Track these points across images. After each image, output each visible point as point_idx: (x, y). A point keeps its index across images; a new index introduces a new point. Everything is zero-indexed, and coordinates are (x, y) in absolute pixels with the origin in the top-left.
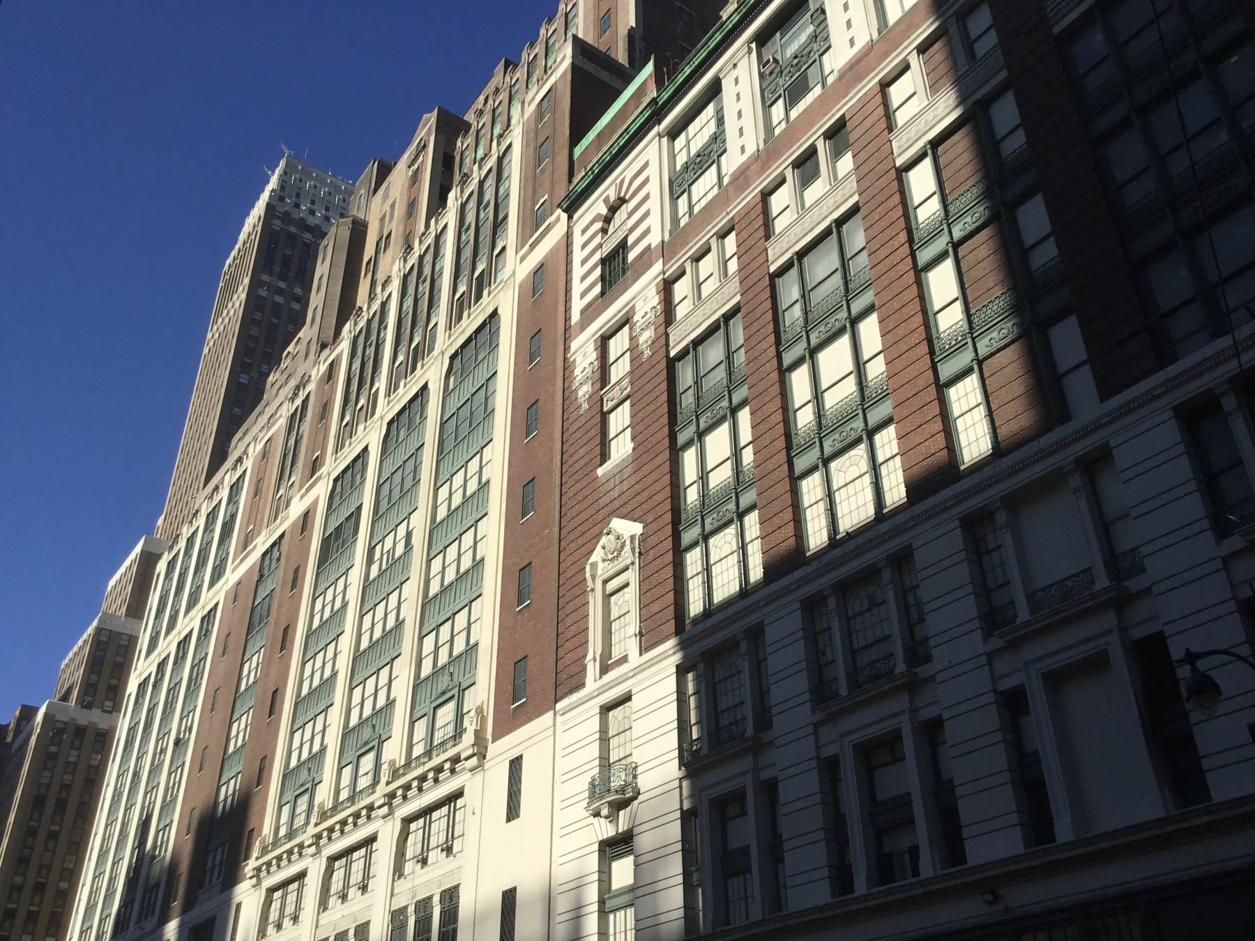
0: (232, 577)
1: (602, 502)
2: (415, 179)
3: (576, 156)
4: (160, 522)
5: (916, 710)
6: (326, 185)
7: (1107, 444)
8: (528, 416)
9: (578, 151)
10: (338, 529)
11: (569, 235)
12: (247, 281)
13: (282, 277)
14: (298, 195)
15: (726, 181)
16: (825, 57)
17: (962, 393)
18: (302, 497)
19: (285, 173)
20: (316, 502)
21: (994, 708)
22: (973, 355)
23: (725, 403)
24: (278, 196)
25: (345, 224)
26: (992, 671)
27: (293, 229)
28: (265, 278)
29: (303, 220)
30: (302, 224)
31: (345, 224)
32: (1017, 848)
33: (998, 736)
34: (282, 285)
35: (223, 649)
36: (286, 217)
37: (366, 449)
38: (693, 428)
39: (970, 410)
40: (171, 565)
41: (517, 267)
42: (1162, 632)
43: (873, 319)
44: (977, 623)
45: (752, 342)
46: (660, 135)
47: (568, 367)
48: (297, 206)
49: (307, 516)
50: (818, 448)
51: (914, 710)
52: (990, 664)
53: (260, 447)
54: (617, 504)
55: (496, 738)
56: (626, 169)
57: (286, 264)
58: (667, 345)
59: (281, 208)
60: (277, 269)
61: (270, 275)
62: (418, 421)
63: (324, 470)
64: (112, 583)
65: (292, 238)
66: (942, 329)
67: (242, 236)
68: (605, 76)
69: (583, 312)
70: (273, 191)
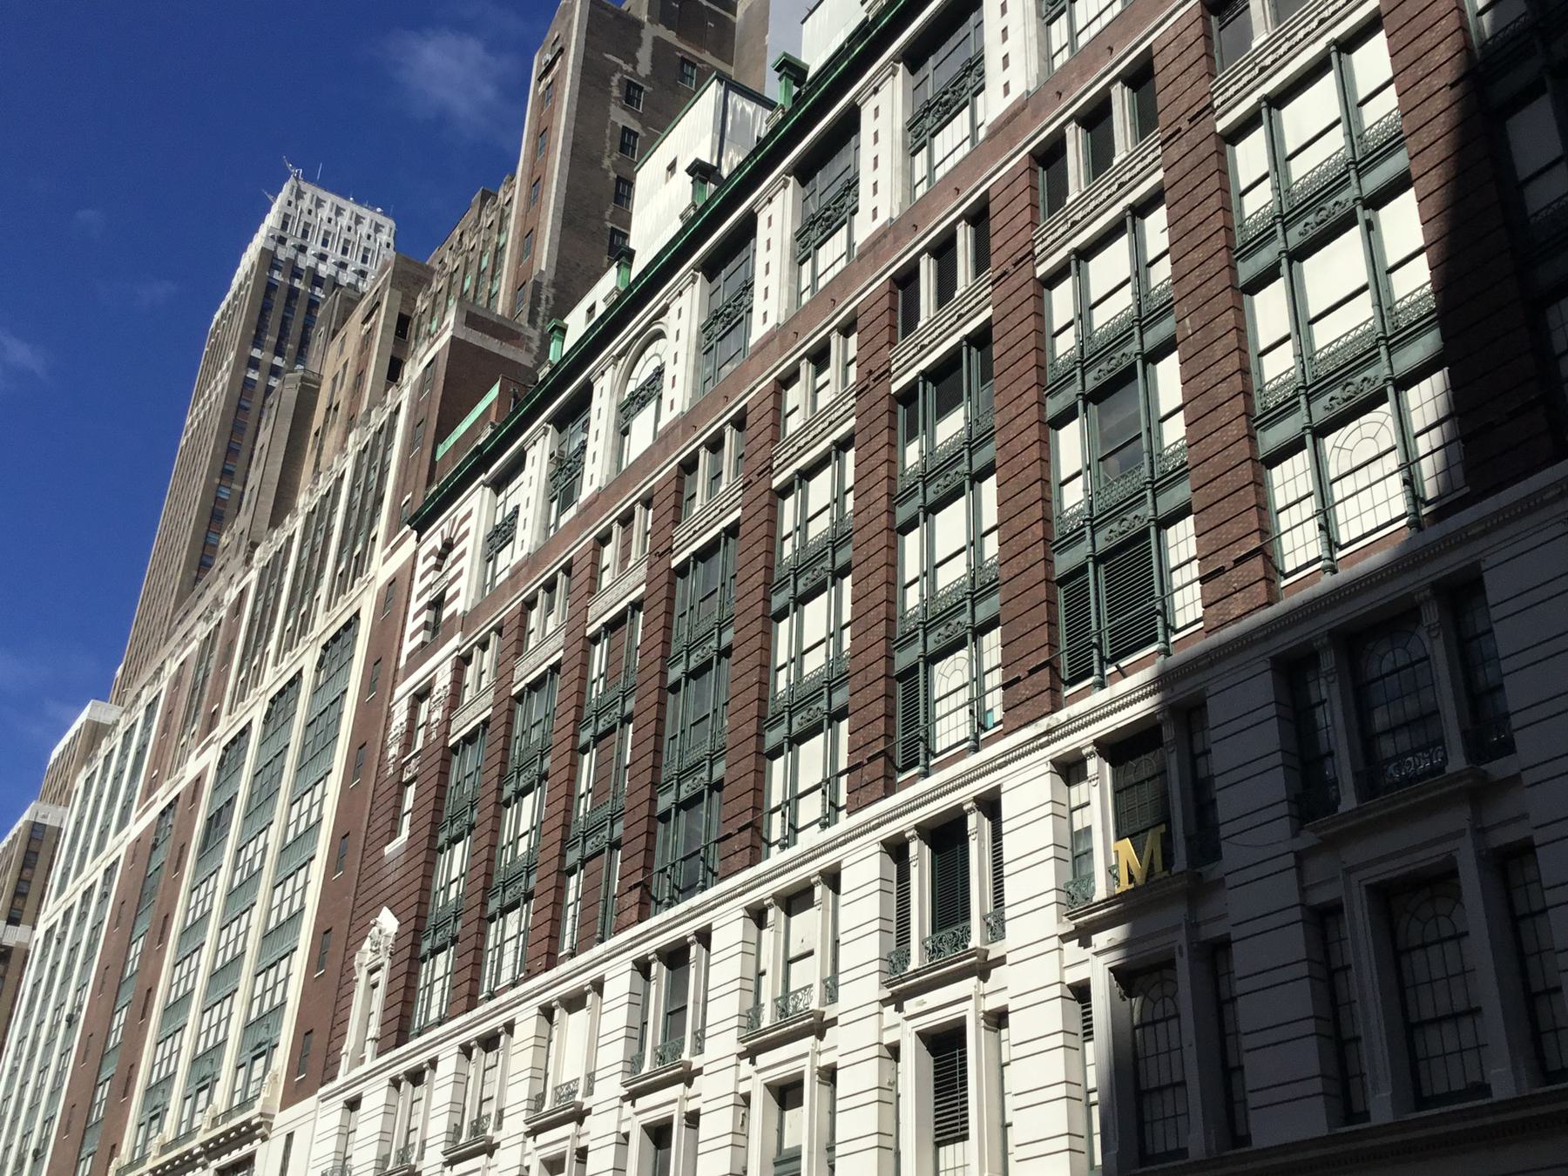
0: (135, 829)
1: (383, 884)
2: (366, 340)
3: (438, 457)
4: (119, 672)
5: (1197, 925)
7: (1476, 566)
8: (355, 766)
9: (442, 450)
10: (219, 811)
11: (416, 553)
12: (232, 355)
15: (982, 133)
16: (821, 251)
17: (1289, 476)
18: (198, 756)
20: (206, 769)
21: (1298, 930)
22: (1090, 549)
23: (827, 564)
25: (292, 380)
26: (1300, 879)
31: (292, 380)
32: (1321, 1129)
35: (117, 920)
37: (300, 673)
38: (789, 591)
39: (1298, 501)
40: (89, 781)
41: (381, 570)
42: (1530, 838)
43: (1173, 361)
44: (1284, 809)
45: (865, 485)
46: (484, 484)
47: (389, 716)
49: (199, 780)
50: (786, 724)
51: (1193, 926)
52: (1299, 866)
53: (175, 666)
54: (389, 892)
56: (459, 509)
58: (447, 733)
62: (280, 721)
63: (218, 732)
64: (55, 754)
66: (1267, 377)
67: (235, 283)
69: (409, 657)
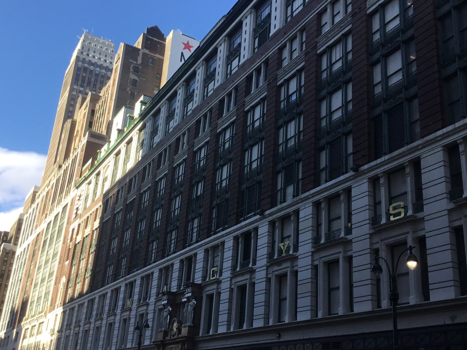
6: (100, 43)
13: (82, 86)
14: (89, 50)
19: (84, 41)
24: (81, 52)
27: (86, 65)
28: (75, 87)
29: (90, 61)
30: (90, 63)
33: (449, 247)
34: (82, 89)
36: (84, 61)
48: (88, 55)
55: (49, 312)
57: (83, 81)
59: (82, 57)
60: (80, 83)
61: (77, 85)
65: (85, 69)
68: (97, 141)
70: (79, 50)
